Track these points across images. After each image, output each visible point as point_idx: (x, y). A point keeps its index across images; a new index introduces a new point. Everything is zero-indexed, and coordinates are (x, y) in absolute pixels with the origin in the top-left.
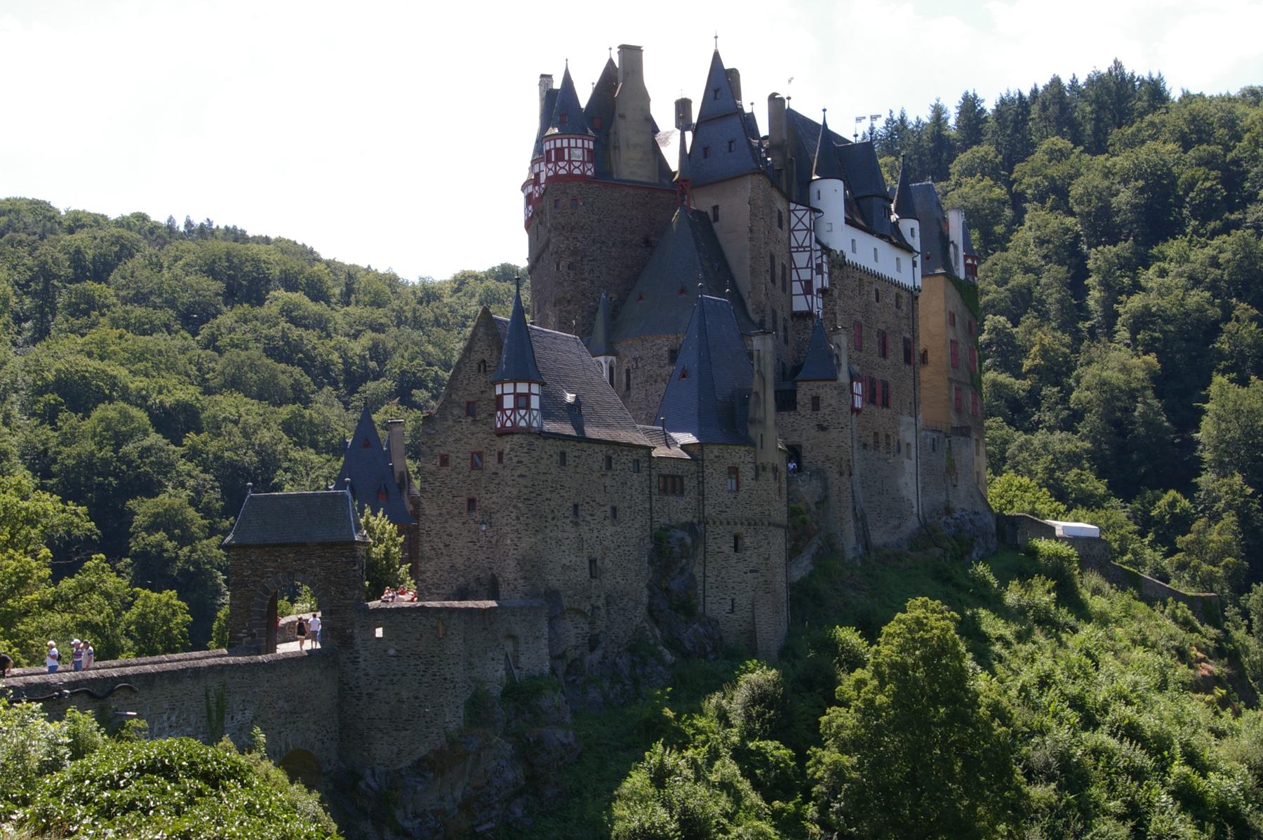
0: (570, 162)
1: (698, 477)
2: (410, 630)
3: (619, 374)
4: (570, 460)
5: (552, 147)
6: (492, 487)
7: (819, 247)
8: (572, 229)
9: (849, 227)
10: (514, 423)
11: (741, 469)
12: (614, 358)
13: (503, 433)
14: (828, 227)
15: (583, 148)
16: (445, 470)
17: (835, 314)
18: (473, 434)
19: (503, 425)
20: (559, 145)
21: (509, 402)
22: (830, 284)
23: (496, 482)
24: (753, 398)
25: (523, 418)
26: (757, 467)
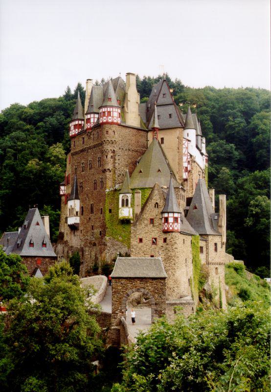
0: (113, 117)
2: (185, 311)
5: (106, 110)
7: (189, 154)
8: (113, 143)
9: (196, 149)
10: (173, 229)
13: (166, 232)
16: (141, 244)
17: (193, 180)
18: (153, 231)
19: (168, 229)
20: (109, 110)
21: (171, 220)
22: (192, 169)
24: (220, 218)
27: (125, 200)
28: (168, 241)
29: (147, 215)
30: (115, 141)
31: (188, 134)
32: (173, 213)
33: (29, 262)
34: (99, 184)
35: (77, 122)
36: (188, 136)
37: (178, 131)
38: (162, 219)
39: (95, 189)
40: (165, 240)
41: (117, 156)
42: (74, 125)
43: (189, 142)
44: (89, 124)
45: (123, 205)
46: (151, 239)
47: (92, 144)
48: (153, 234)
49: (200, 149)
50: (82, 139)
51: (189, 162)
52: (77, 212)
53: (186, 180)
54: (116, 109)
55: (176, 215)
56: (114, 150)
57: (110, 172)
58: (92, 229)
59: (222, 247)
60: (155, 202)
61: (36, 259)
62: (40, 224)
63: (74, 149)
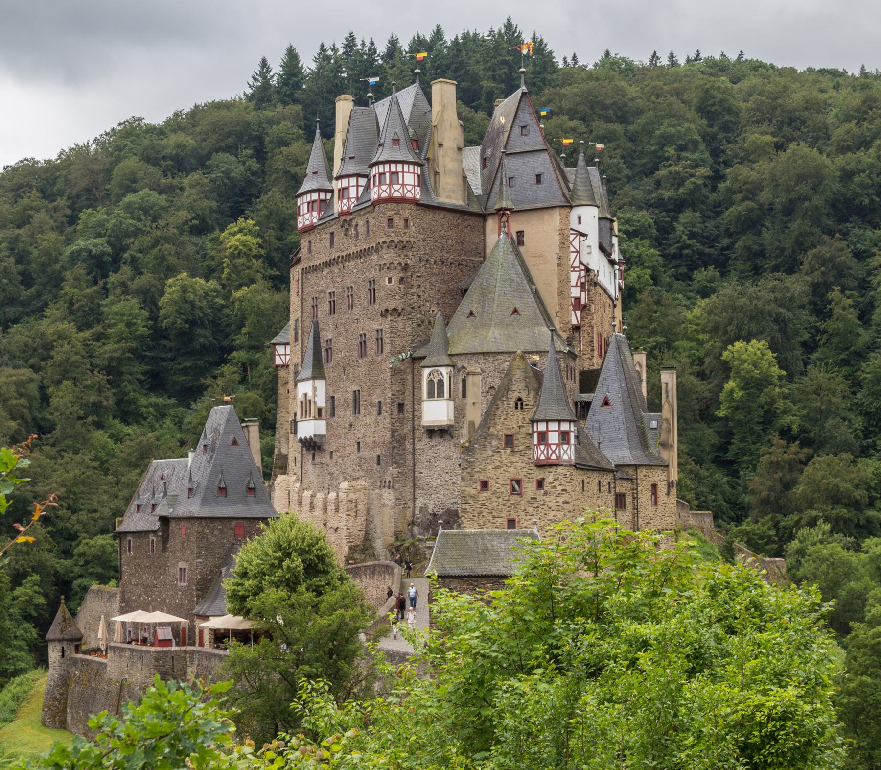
0: (403, 185)
1: (633, 493)
3: (456, 383)
4: (586, 485)
5: (387, 169)
6: (530, 510)
7: (582, 267)
8: (404, 247)
10: (559, 457)
11: (659, 486)
12: (451, 369)
13: (540, 466)
14: (588, 250)
15: (414, 173)
16: (485, 494)
17: (592, 327)
18: (512, 463)
19: (548, 458)
21: (554, 438)
22: (590, 301)
23: (535, 505)
24: (665, 425)
25: (565, 452)
26: (669, 483)
27: (436, 381)
28: (547, 486)
29: (500, 428)
30: (408, 242)
31: (579, 218)
32: (559, 421)
33: (216, 532)
34: (371, 345)
35: (315, 196)
36: (580, 223)
37: (557, 215)
38: (531, 435)
39: (363, 354)
40: (540, 484)
41: (414, 278)
42: (309, 203)
43: (582, 238)
44: (345, 201)
45: (431, 395)
46: (509, 481)
47: (354, 249)
48: (512, 469)
49: (609, 250)
50: (328, 236)
51: (582, 285)
52: (320, 410)
53: (577, 328)
54: (411, 167)
55: (565, 427)
56: (406, 264)
57: (399, 315)
58: (359, 450)
59: (668, 494)
60: (516, 395)
61: (233, 523)
62: (239, 442)
63: (309, 259)
